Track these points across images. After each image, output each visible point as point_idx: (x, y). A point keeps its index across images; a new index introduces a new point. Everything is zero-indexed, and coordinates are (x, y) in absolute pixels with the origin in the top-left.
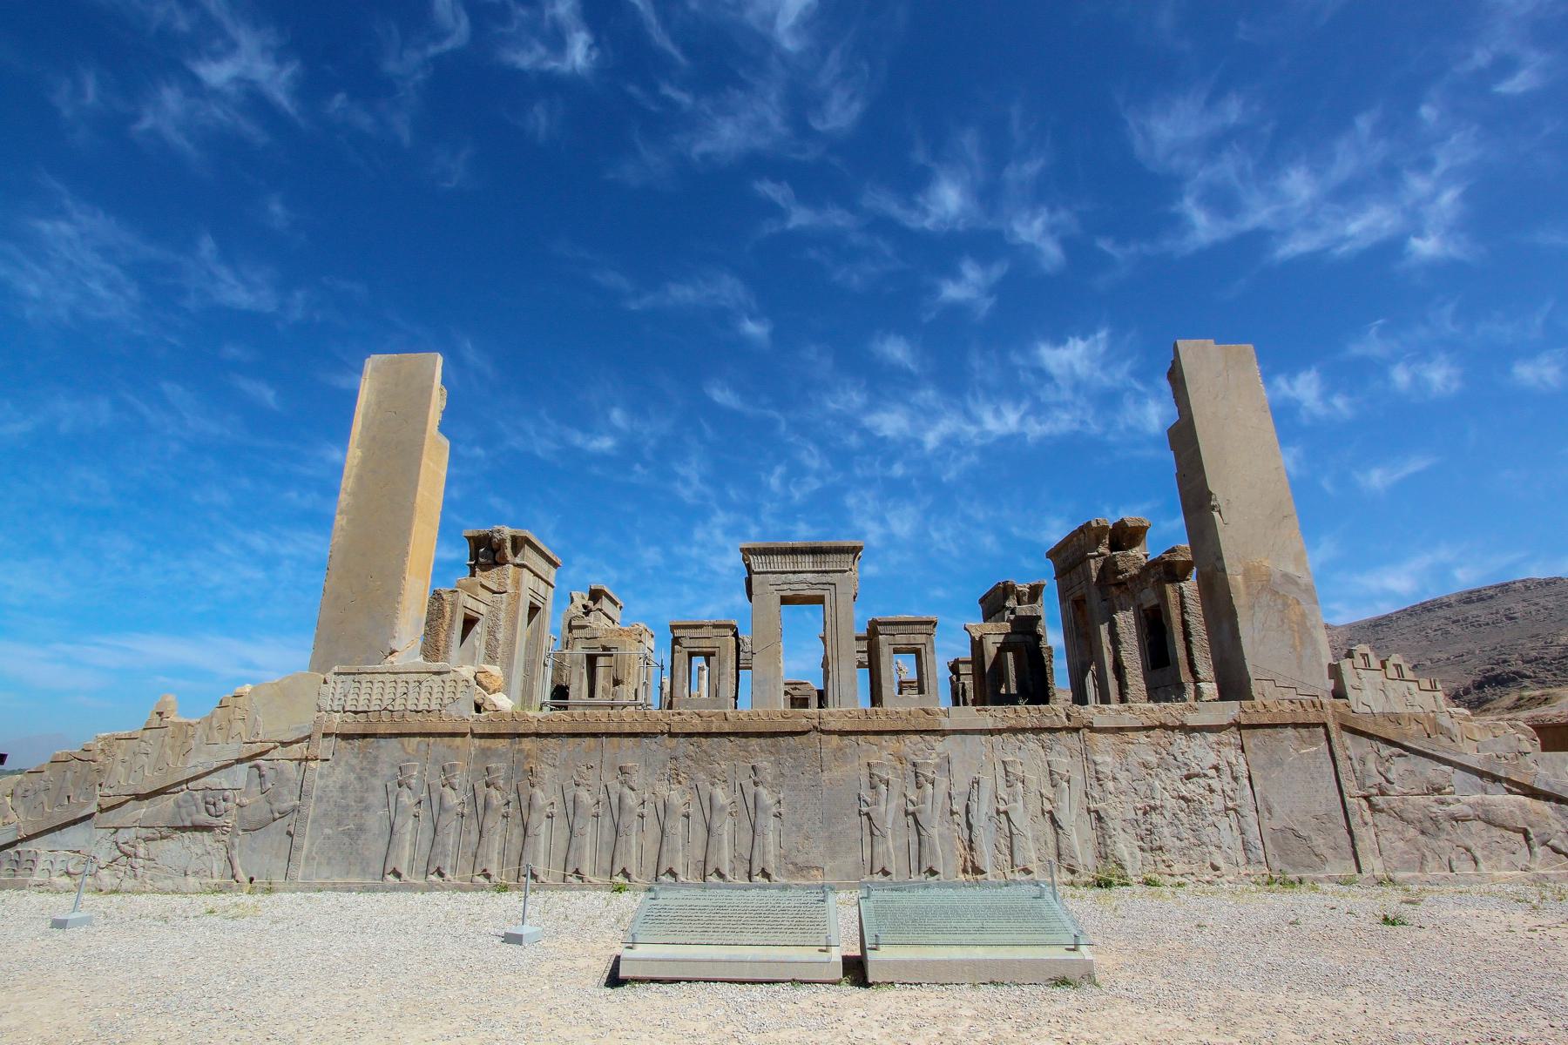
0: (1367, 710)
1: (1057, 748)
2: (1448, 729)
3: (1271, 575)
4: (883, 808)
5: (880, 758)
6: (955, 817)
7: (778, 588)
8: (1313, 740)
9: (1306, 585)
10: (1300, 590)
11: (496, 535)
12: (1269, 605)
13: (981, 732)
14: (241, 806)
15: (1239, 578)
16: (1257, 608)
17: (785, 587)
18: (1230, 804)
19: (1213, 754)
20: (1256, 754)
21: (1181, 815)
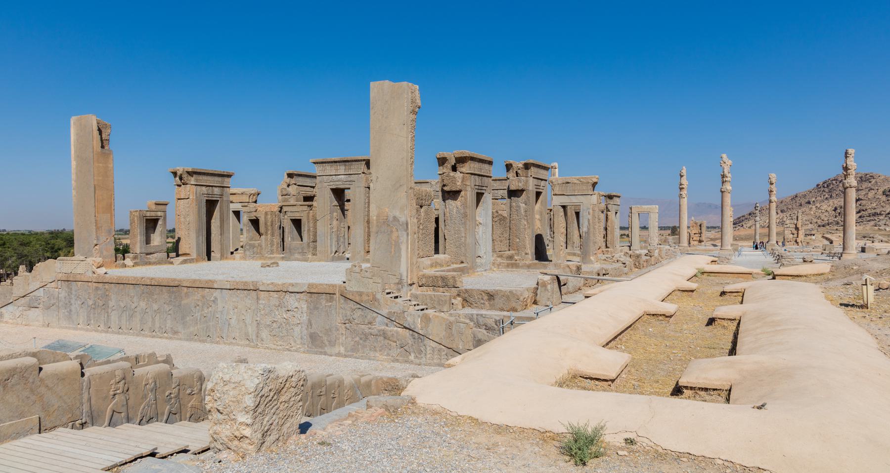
0: (351, 289)
1: (249, 297)
2: (378, 300)
3: (388, 217)
4: (196, 315)
5: (198, 297)
6: (217, 319)
7: (329, 184)
8: (331, 300)
9: (402, 222)
10: (399, 224)
11: (178, 172)
12: (384, 232)
13: (227, 289)
14: (43, 302)
15: (375, 218)
16: (379, 233)
17: (332, 183)
18: (298, 322)
19: (296, 304)
20: (310, 304)
21: (284, 324)
